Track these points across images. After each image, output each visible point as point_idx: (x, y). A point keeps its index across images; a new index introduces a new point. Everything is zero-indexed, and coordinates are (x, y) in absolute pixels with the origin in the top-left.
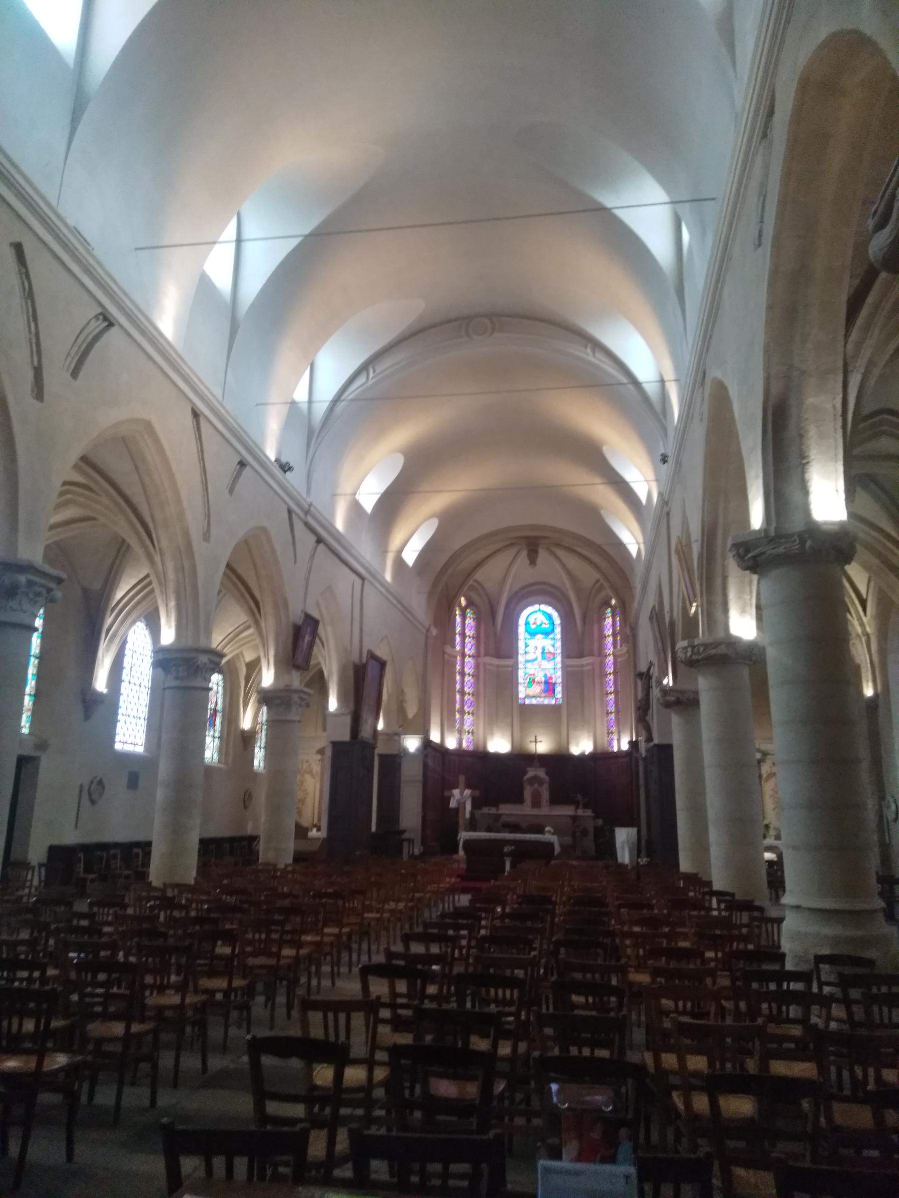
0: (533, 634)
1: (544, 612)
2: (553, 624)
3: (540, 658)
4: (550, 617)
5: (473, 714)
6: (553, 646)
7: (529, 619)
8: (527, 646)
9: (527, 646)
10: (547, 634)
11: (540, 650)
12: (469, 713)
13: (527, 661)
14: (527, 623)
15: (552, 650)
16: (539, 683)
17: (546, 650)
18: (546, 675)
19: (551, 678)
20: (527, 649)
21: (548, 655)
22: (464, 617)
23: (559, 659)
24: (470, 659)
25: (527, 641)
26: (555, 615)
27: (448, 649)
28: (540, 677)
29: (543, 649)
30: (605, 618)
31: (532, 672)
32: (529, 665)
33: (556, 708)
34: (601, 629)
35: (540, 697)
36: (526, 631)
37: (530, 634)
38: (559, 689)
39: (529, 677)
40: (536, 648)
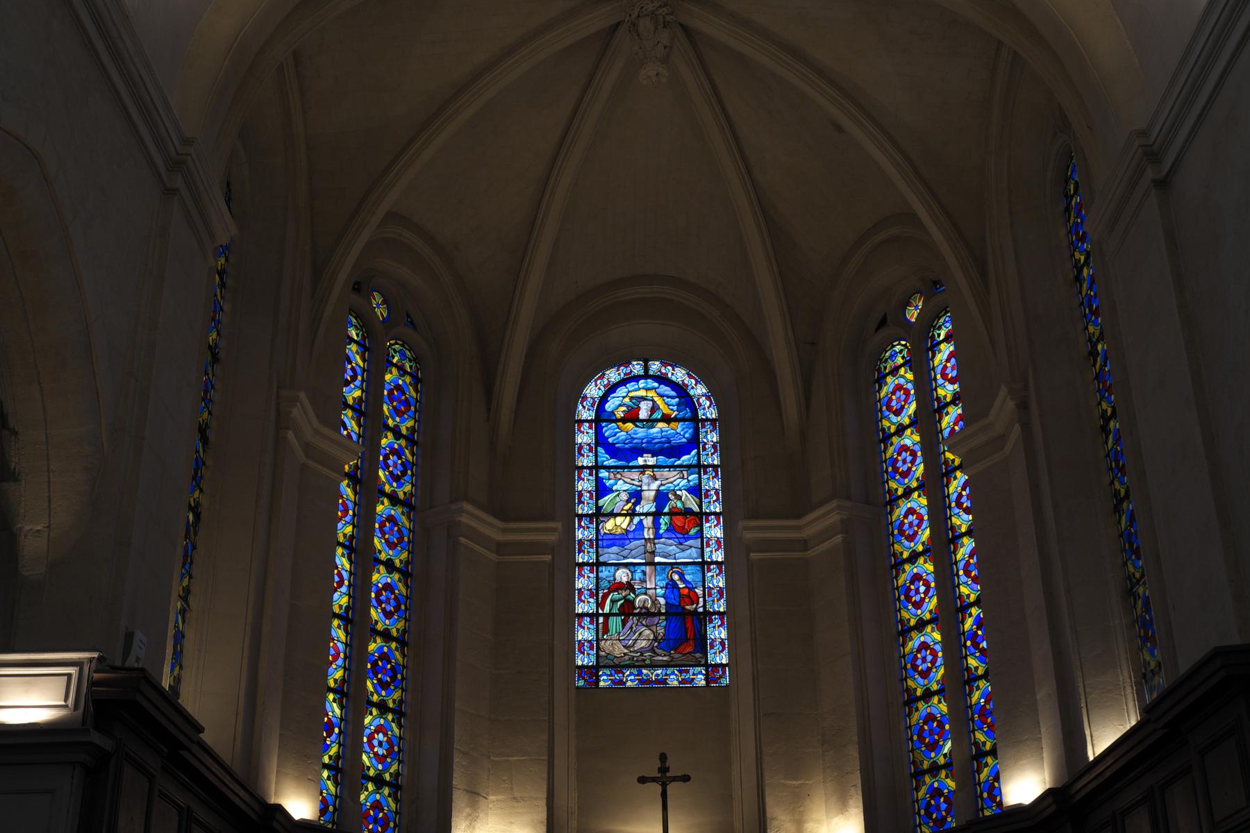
0: (626, 454)
1: (662, 379)
2: (695, 421)
3: (648, 534)
4: (680, 390)
5: (399, 713)
6: (696, 491)
7: (609, 406)
8: (602, 490)
9: (602, 490)
10: (672, 450)
11: (647, 506)
12: (382, 707)
13: (601, 541)
14: (602, 416)
15: (692, 504)
16: (646, 614)
17: (674, 503)
18: (671, 585)
19: (693, 599)
20: (605, 501)
21: (679, 521)
22: (377, 363)
23: (714, 531)
24: (397, 512)
25: (603, 474)
26: (699, 391)
27: (303, 412)
28: (653, 590)
29: (661, 498)
30: (881, 380)
31: (622, 575)
32: (610, 555)
33: (715, 698)
34: (871, 411)
35: (653, 666)
36: (601, 440)
37: (612, 451)
38: (717, 633)
39: (615, 595)
40: (636, 496)
